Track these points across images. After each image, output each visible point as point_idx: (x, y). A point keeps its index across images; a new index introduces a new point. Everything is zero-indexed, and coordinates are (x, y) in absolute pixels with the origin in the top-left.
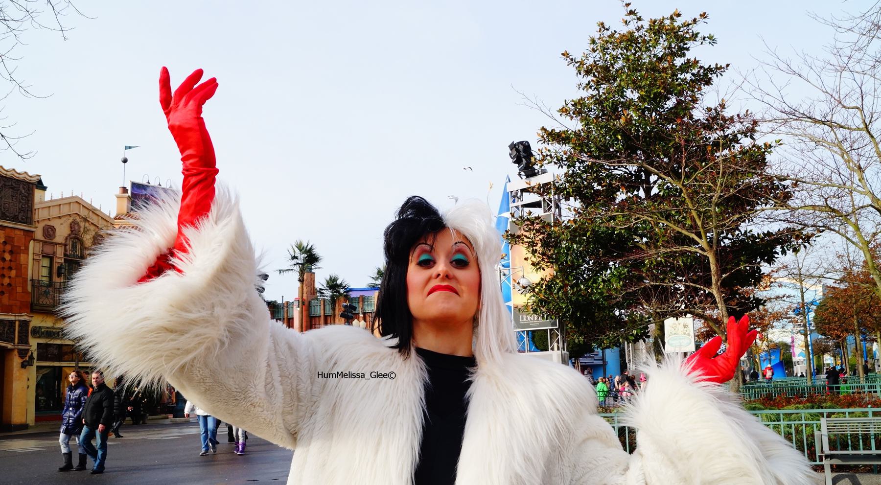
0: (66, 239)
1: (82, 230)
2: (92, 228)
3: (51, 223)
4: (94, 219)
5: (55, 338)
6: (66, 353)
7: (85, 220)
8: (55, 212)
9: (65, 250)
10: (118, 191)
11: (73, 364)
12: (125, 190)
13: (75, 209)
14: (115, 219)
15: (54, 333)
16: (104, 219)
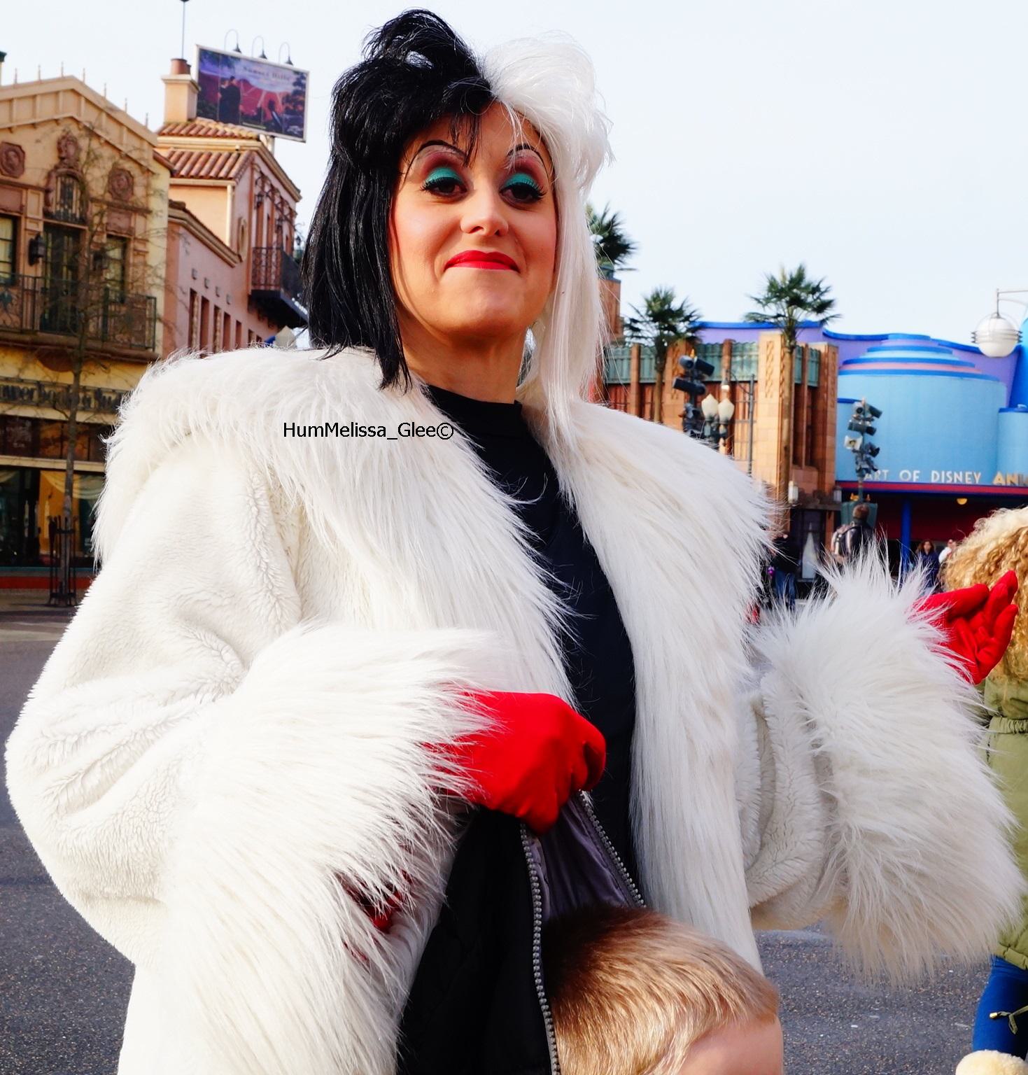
0: (49, 176)
1: (83, 156)
2: (107, 152)
3: (15, 139)
4: (110, 132)
5: (24, 404)
6: (47, 443)
7: (91, 133)
8: (23, 114)
9: (47, 203)
10: (168, 69)
11: (62, 464)
12: (183, 66)
13: (68, 107)
14: (161, 134)
15: (22, 393)
16: (135, 132)
